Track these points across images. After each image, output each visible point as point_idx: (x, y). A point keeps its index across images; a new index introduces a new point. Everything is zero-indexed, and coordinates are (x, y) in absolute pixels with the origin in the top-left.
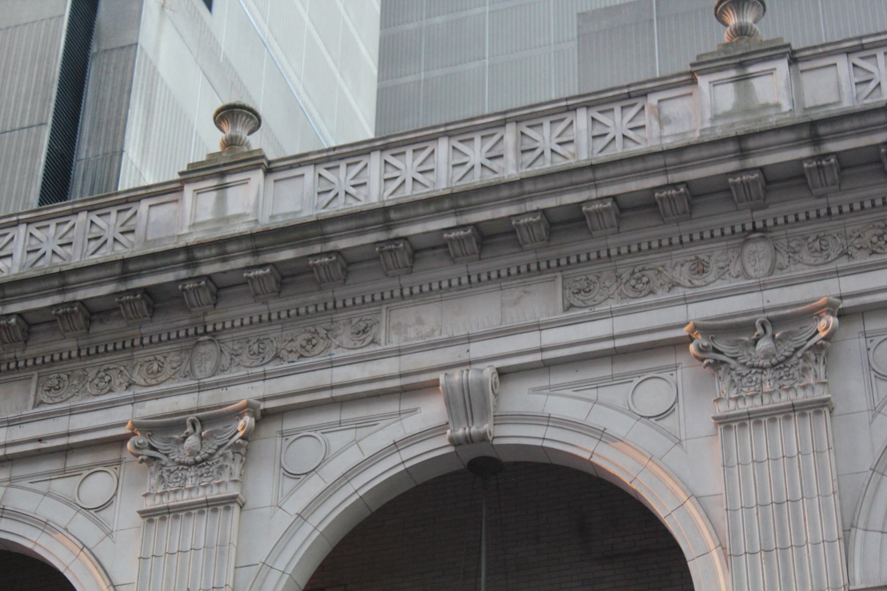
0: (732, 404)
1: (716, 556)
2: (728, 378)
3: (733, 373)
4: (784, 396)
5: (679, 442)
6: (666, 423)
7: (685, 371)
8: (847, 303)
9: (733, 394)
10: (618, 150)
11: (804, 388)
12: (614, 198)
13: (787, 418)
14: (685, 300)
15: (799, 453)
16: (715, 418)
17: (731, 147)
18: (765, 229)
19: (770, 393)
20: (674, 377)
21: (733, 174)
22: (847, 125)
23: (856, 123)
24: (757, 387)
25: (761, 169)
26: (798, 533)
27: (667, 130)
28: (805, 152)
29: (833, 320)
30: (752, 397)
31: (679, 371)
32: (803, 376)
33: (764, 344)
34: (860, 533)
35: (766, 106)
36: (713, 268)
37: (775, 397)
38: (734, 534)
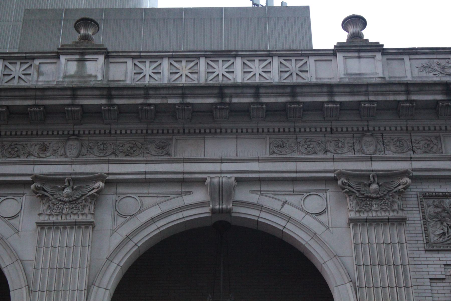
0: (47, 217)
1: (25, 291)
2: (47, 205)
3: (50, 202)
4: (72, 217)
5: (18, 232)
6: (13, 221)
7: (27, 198)
8: (110, 177)
9: (48, 212)
10: (15, 83)
11: (83, 214)
12: (8, 107)
13: (72, 228)
14: (34, 163)
15: (74, 245)
16: (37, 223)
17: (69, 93)
18: (78, 135)
19: (66, 215)
20: (21, 200)
21: (68, 105)
22: (125, 92)
23: (130, 92)
24: (61, 210)
25: (82, 106)
26: (66, 284)
27: (41, 78)
28: (103, 102)
29: (101, 184)
30: (57, 215)
31: (24, 197)
32: (83, 209)
33: (67, 191)
34: (95, 288)
35: (90, 76)
36: (51, 149)
37: (68, 217)
38: (35, 280)
